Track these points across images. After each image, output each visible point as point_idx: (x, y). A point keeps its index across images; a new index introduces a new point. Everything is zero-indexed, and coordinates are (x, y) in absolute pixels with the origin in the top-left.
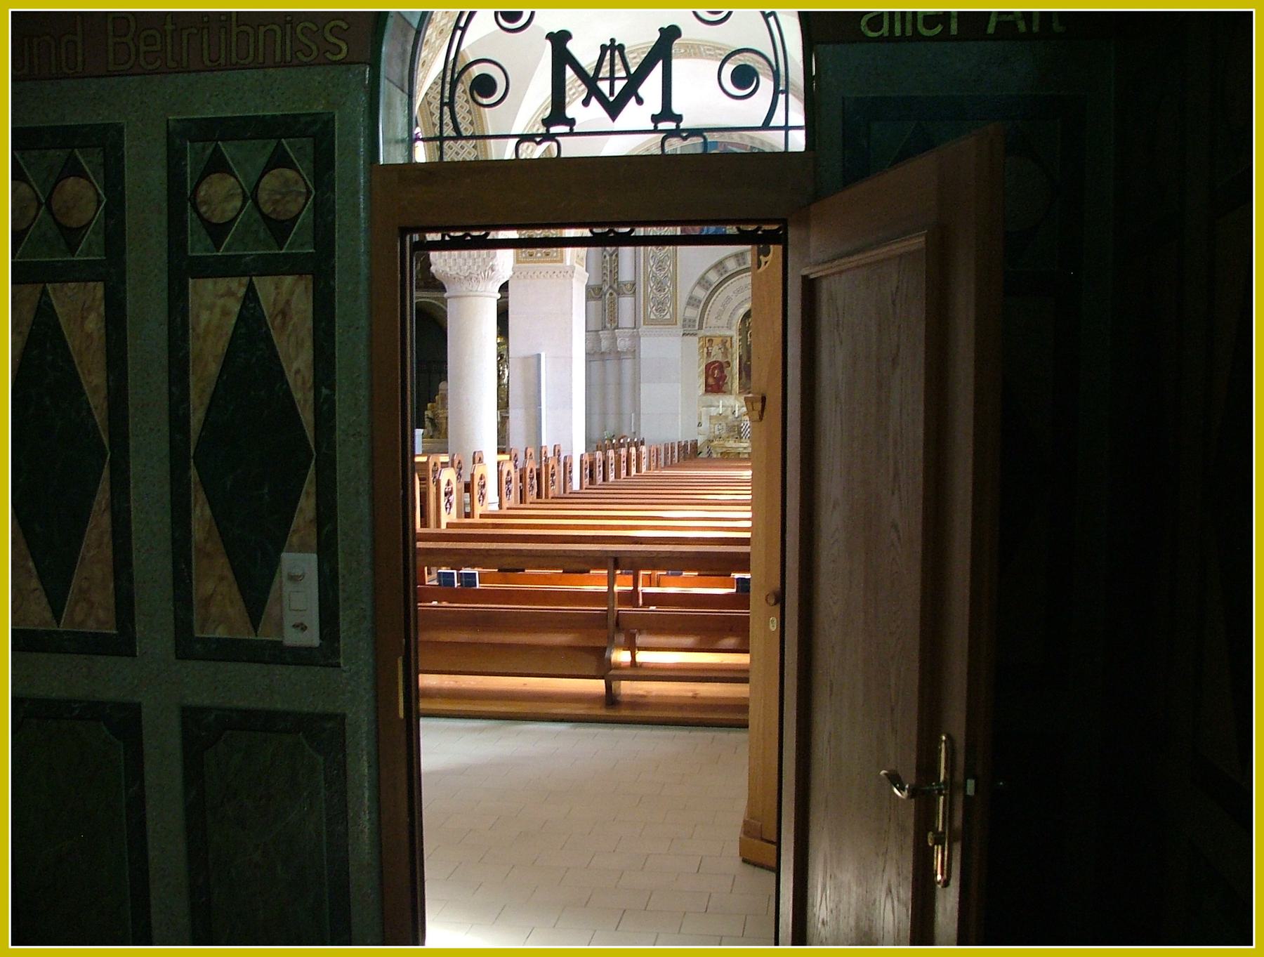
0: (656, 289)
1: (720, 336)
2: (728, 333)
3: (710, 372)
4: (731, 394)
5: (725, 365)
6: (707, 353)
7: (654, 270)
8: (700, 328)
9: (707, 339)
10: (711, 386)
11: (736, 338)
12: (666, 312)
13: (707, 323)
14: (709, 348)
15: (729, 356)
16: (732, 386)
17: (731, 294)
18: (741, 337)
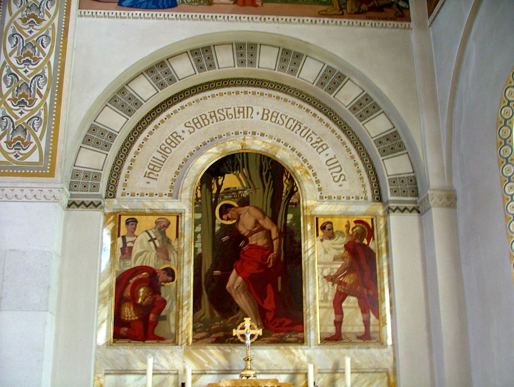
0: (14, 100)
1: (153, 213)
2: (172, 205)
3: (127, 293)
4: (175, 343)
5: (162, 276)
6: (123, 250)
7: (14, 61)
8: (111, 193)
9: (124, 219)
10: (128, 324)
11: (188, 217)
12: (31, 146)
13: (125, 185)
14: (128, 239)
15: (173, 257)
16: (177, 327)
17: (179, 130)
18: (199, 216)
